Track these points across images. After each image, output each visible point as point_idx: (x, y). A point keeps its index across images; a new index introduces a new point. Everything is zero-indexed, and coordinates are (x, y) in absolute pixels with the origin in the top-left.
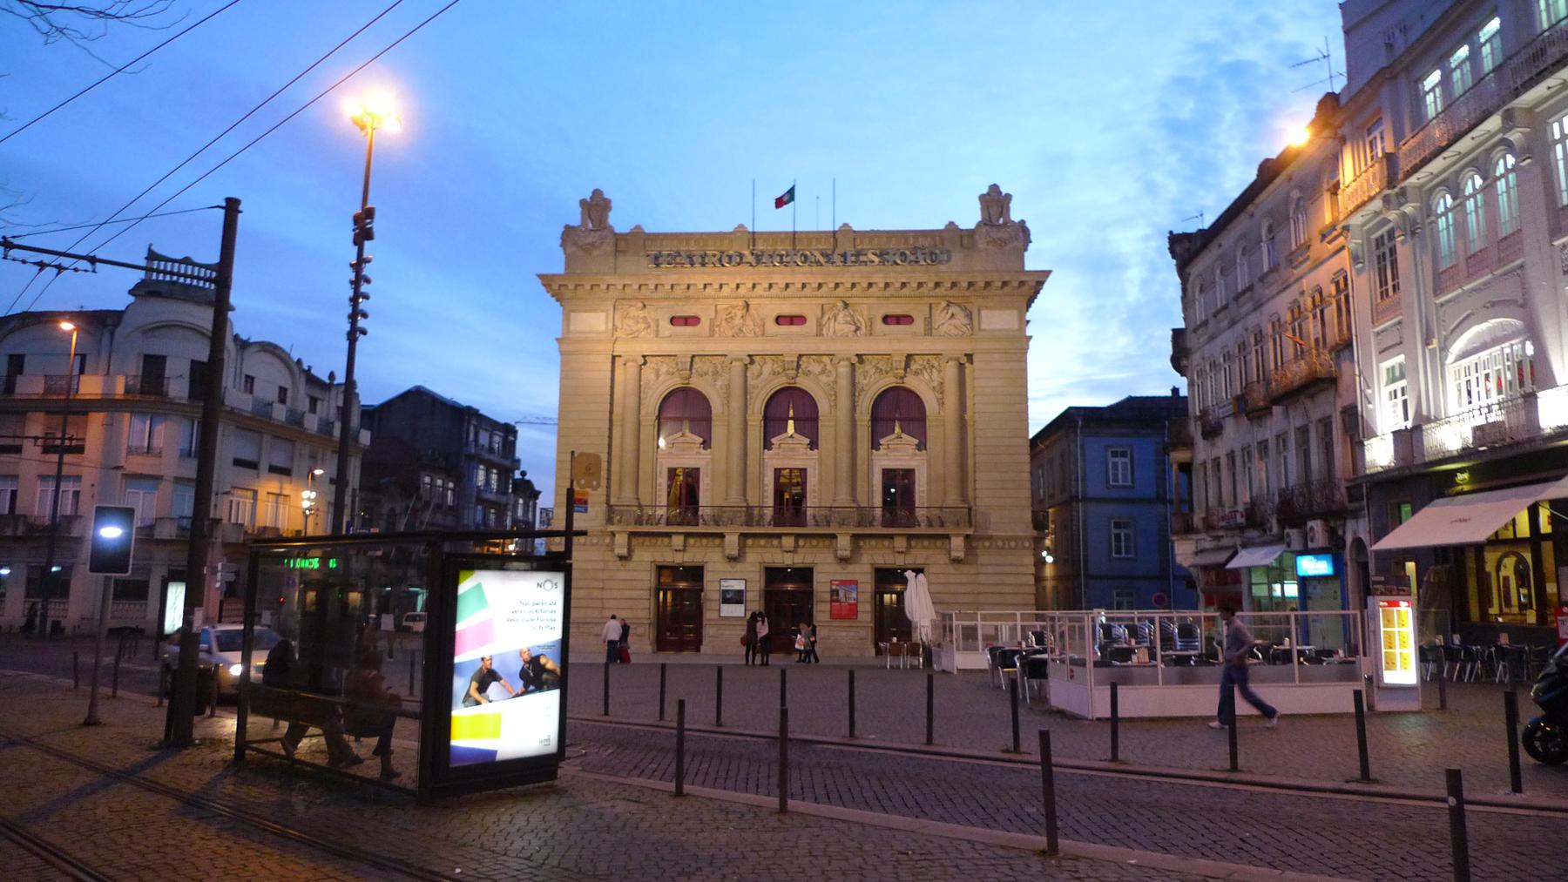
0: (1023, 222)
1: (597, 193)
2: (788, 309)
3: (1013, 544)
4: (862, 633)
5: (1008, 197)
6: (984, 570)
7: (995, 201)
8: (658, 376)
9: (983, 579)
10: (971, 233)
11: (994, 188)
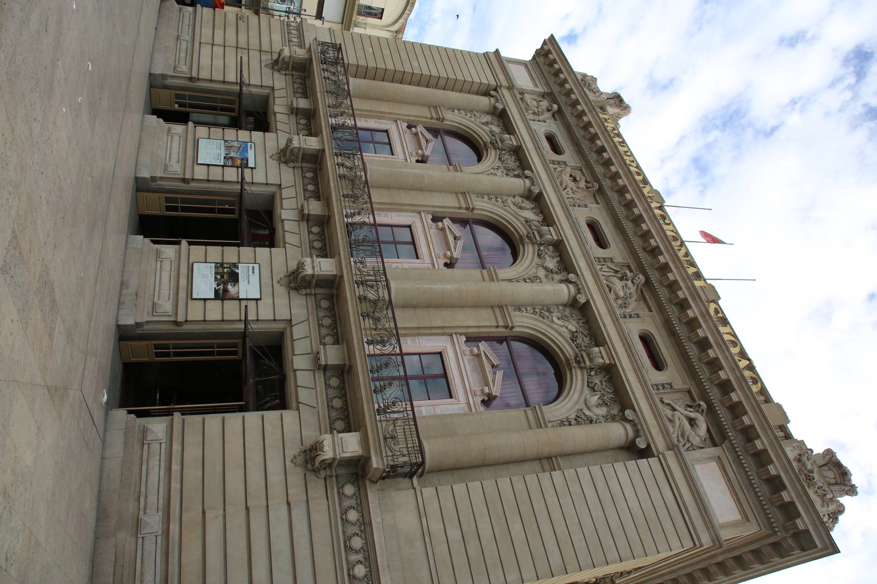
2: (608, 230)
4: (166, 306)
6: (299, 513)
9: (279, 513)
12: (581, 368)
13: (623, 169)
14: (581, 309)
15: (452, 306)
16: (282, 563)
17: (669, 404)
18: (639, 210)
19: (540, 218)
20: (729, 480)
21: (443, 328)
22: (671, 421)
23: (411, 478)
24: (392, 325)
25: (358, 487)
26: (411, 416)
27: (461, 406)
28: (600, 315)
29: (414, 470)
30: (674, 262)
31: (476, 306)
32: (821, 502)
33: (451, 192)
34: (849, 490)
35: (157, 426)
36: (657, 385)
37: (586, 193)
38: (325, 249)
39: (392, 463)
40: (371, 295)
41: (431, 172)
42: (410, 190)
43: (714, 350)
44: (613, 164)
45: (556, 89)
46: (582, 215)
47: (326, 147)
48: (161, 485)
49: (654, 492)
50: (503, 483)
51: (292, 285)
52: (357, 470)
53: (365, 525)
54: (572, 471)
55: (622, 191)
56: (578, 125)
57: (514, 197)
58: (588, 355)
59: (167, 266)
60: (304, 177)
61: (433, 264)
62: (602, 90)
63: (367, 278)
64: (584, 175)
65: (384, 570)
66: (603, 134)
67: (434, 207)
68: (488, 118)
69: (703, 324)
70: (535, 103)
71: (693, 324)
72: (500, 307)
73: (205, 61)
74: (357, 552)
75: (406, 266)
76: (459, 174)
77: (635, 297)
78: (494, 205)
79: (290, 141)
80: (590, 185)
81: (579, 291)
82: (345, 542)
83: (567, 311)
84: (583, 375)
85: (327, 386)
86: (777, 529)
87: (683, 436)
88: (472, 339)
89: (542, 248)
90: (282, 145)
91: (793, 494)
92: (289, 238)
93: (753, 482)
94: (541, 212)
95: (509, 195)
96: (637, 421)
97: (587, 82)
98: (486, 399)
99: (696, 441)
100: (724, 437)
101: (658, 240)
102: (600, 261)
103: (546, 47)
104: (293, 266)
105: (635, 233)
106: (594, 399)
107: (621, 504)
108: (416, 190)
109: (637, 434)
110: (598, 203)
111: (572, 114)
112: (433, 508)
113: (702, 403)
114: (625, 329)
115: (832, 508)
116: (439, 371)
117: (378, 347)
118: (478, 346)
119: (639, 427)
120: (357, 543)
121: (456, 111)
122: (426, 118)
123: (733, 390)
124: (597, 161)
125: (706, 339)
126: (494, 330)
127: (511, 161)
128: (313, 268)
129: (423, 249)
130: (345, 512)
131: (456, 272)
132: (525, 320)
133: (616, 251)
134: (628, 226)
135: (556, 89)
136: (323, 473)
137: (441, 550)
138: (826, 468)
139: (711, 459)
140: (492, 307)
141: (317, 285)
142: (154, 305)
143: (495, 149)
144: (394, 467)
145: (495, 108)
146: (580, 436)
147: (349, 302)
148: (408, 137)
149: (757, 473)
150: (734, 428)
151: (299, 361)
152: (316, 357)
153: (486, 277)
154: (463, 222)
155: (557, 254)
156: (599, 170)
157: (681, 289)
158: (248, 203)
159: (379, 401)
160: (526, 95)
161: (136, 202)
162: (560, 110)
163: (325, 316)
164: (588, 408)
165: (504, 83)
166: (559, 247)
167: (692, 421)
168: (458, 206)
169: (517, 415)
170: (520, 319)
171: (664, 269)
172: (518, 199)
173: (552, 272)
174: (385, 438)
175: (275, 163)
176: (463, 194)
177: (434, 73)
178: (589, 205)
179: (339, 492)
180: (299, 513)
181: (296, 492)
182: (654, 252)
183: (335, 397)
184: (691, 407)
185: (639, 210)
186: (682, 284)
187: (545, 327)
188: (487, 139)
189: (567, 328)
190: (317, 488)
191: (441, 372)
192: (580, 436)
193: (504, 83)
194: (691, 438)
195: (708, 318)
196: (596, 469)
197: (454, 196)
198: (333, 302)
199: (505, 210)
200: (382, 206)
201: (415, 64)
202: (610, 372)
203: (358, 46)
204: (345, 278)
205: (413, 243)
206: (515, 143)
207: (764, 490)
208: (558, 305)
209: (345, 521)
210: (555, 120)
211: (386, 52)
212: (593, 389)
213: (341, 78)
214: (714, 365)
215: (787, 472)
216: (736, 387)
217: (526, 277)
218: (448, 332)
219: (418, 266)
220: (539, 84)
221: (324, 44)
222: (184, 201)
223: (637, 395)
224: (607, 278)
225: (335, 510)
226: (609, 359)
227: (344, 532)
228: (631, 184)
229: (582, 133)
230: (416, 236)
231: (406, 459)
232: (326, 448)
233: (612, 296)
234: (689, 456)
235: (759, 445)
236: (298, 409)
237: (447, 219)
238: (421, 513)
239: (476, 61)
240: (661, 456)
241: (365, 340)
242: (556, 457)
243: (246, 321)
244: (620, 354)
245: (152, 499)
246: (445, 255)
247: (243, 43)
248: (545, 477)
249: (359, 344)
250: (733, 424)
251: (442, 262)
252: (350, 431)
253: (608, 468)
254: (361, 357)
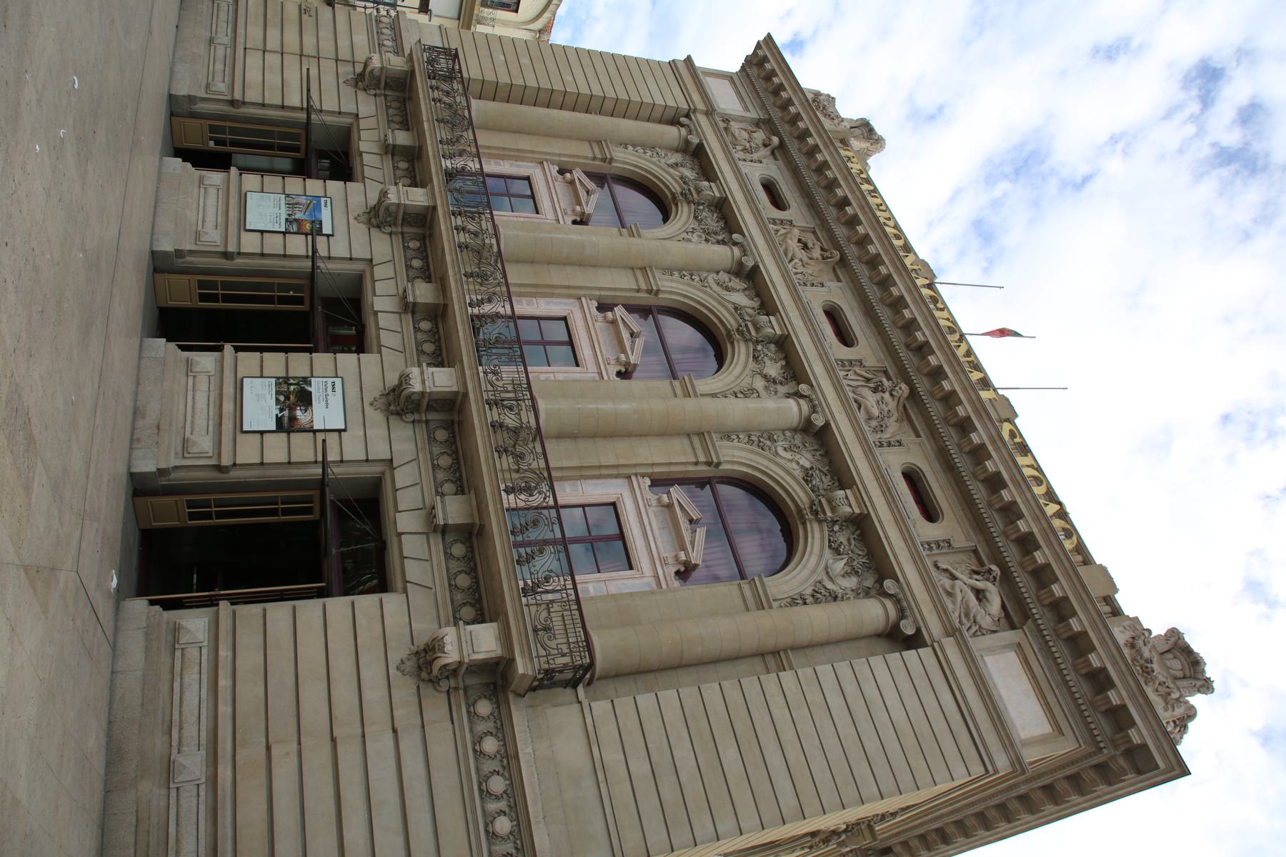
2: (855, 320)
3: (503, 825)
6: (411, 744)
8: (675, 166)
9: (381, 744)
12: (820, 521)
13: (875, 230)
14: (818, 436)
15: (628, 435)
16: (387, 818)
17: (946, 570)
18: (899, 289)
19: (756, 304)
20: (1034, 677)
21: (617, 466)
22: (950, 594)
23: (575, 687)
24: (542, 464)
25: (498, 702)
26: (573, 597)
27: (646, 580)
28: (845, 443)
29: (580, 676)
30: (951, 365)
31: (666, 432)
32: (1163, 704)
33: (625, 268)
34: (1202, 686)
35: (195, 623)
36: (928, 543)
37: (822, 266)
38: (441, 355)
39: (546, 666)
40: (510, 420)
41: (594, 238)
42: (564, 264)
43: (1010, 491)
44: (860, 223)
45: (776, 114)
46: (816, 299)
47: (439, 202)
48: (204, 710)
49: (928, 698)
50: (711, 691)
51: (392, 408)
52: (495, 678)
53: (509, 758)
54: (809, 671)
55: (874, 262)
56: (808, 167)
57: (718, 273)
58: (830, 501)
59: (203, 384)
60: (406, 248)
61: (601, 374)
62: (844, 114)
63: (504, 395)
64: (818, 240)
65: (538, 823)
66: (845, 179)
67: (600, 289)
68: (677, 158)
69: (993, 454)
70: (746, 135)
71: (979, 454)
72: (701, 435)
73: (253, 75)
74: (498, 798)
75: (560, 377)
76: (636, 240)
77: (896, 416)
78: (688, 285)
79: (384, 194)
80: (828, 254)
81: (814, 409)
82: (480, 784)
83: (798, 439)
84: (822, 531)
85: (448, 556)
86: (1102, 745)
87: (967, 615)
88: (659, 482)
89: (759, 347)
90: (373, 200)
91: (1124, 694)
92: (385, 338)
93: (1068, 678)
94: (758, 295)
95: (710, 271)
96: (901, 596)
97: (821, 104)
98: (682, 569)
99: (986, 622)
100: (1026, 615)
101: (927, 333)
102: (843, 365)
103: (760, 53)
104: (392, 379)
105: (894, 323)
106: (839, 566)
107: (881, 716)
108: (573, 264)
109: (902, 614)
110: (839, 280)
111: (800, 150)
112: (607, 731)
113: (994, 567)
114: (882, 462)
115: (1179, 711)
116: (614, 530)
117: (522, 497)
118: (668, 493)
119: (905, 604)
120: (497, 784)
121: (630, 148)
122: (587, 158)
123: (1038, 547)
124: (838, 219)
125: (998, 474)
126: (691, 468)
127: (712, 221)
128: (423, 382)
129: (585, 351)
130: (478, 740)
131: (633, 385)
132: (736, 453)
133: (866, 350)
134: (884, 313)
135: (776, 114)
136: (444, 685)
137: (621, 791)
138: (1170, 656)
139: (1006, 647)
140: (688, 435)
141: (430, 408)
142: (185, 441)
143: (689, 203)
144: (549, 673)
145: (687, 142)
146: (819, 619)
147: (478, 432)
148: (560, 187)
149: (1074, 666)
150: (1040, 601)
151: (405, 519)
152: (431, 514)
153: (679, 391)
154: (644, 311)
155: (781, 356)
156: (840, 231)
157: (961, 403)
158: (322, 287)
159: (525, 577)
160: (732, 123)
161: (153, 289)
162: (782, 145)
163: (443, 454)
164: (831, 579)
165: (700, 106)
166: (784, 345)
167: (980, 594)
168: (635, 287)
169: (728, 592)
170: (730, 452)
171: (937, 374)
172: (724, 277)
173: (774, 382)
174: (535, 631)
175: (363, 228)
176: (643, 269)
177: (597, 91)
178: (827, 284)
179: (469, 712)
180: (411, 744)
181: (406, 714)
182: (922, 350)
183: (460, 572)
184: (977, 573)
185: (899, 289)
186: (962, 396)
187: (766, 463)
188: (677, 188)
189: (798, 463)
190: (436, 706)
191: (616, 531)
192: (819, 619)
193: (700, 106)
194: (979, 618)
195: (1000, 444)
196: (843, 668)
197: (629, 273)
198: (453, 433)
199: (705, 293)
200: (523, 290)
201: (568, 78)
202: (861, 526)
203: (484, 52)
204: (471, 395)
205: (571, 343)
206: (717, 195)
207: (1083, 689)
208: (784, 431)
209: (479, 754)
210: (776, 159)
211: (525, 61)
212: (837, 552)
213: (458, 99)
214: (1010, 512)
215: (1115, 664)
216: (1041, 542)
217: (737, 390)
218: (624, 473)
219: (578, 376)
220: (750, 107)
221: (431, 48)
222: (226, 285)
223: (901, 558)
224: (854, 389)
225: (464, 738)
226: (860, 507)
227: (478, 770)
228: (887, 252)
229: (815, 178)
230: (574, 332)
231: (567, 660)
232: (448, 648)
233: (862, 416)
234: (977, 644)
235: (1075, 625)
236: (405, 591)
237: (620, 307)
238: (591, 738)
239: (658, 73)
240: (936, 645)
241: (502, 487)
242: (785, 650)
243: (325, 464)
244: (875, 500)
245: (190, 731)
246: (618, 360)
247: (309, 48)
248: (770, 681)
249: (493, 493)
250: (1038, 597)
251: (613, 369)
252: (483, 621)
253: (860, 664)
254: (496, 511)
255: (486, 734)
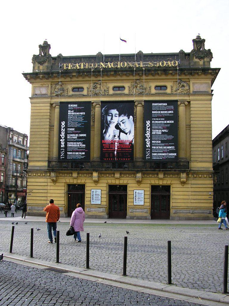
0: (209, 50)
1: (46, 43)
5: (204, 40)
7: (199, 42)
10: (188, 55)
11: (199, 37)
85: (167, 177)
100: (189, 79)
167: (183, 86)
181: (189, 186)
190: (190, 182)
193: (49, 100)
201: (43, 133)
255: (194, 176)
